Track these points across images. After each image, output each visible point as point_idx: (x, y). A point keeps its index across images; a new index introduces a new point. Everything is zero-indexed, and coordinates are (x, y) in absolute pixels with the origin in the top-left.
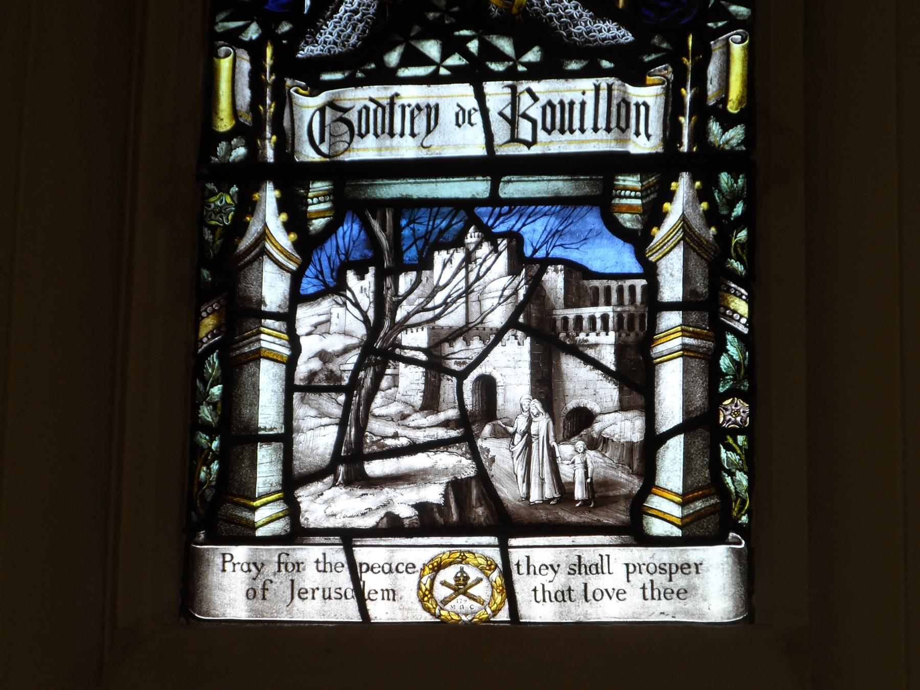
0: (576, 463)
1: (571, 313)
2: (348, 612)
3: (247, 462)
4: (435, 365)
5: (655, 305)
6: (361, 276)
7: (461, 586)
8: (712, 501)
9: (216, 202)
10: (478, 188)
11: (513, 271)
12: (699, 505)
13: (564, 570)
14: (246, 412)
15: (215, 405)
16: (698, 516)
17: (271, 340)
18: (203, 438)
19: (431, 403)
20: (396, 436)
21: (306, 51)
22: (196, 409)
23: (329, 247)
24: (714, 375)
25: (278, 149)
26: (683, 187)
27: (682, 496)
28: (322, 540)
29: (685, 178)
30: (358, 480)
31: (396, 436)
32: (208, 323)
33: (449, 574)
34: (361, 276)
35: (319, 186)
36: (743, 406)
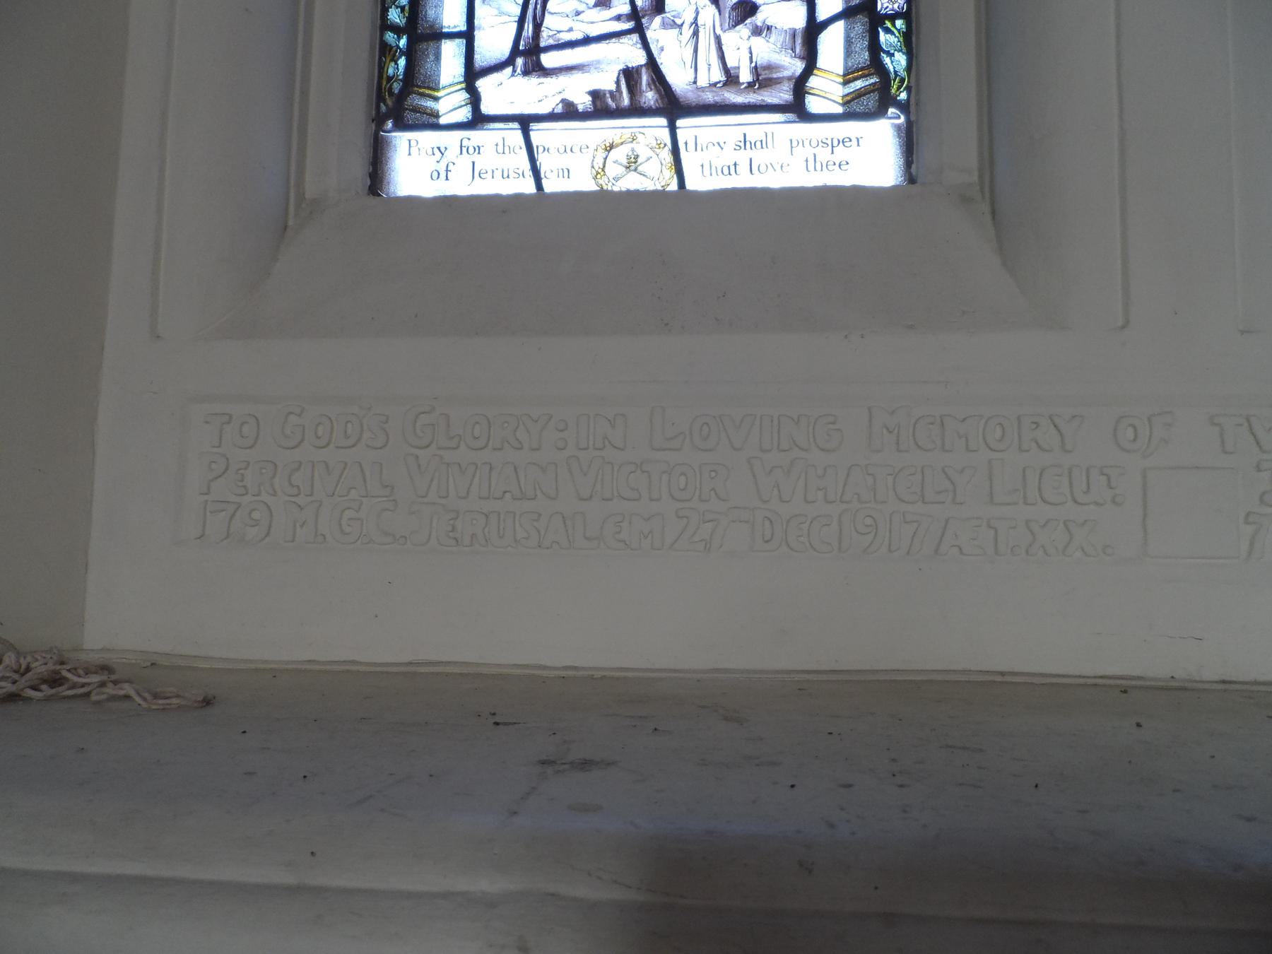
0: (743, 49)
3: (432, 57)
7: (632, 164)
8: (872, 81)
12: (859, 84)
13: (729, 147)
14: (431, 13)
15: (403, 9)
16: (859, 94)
18: (390, 37)
20: (571, 30)
22: (385, 11)
27: (844, 75)
28: (501, 125)
30: (535, 68)
31: (571, 30)
33: (620, 154)
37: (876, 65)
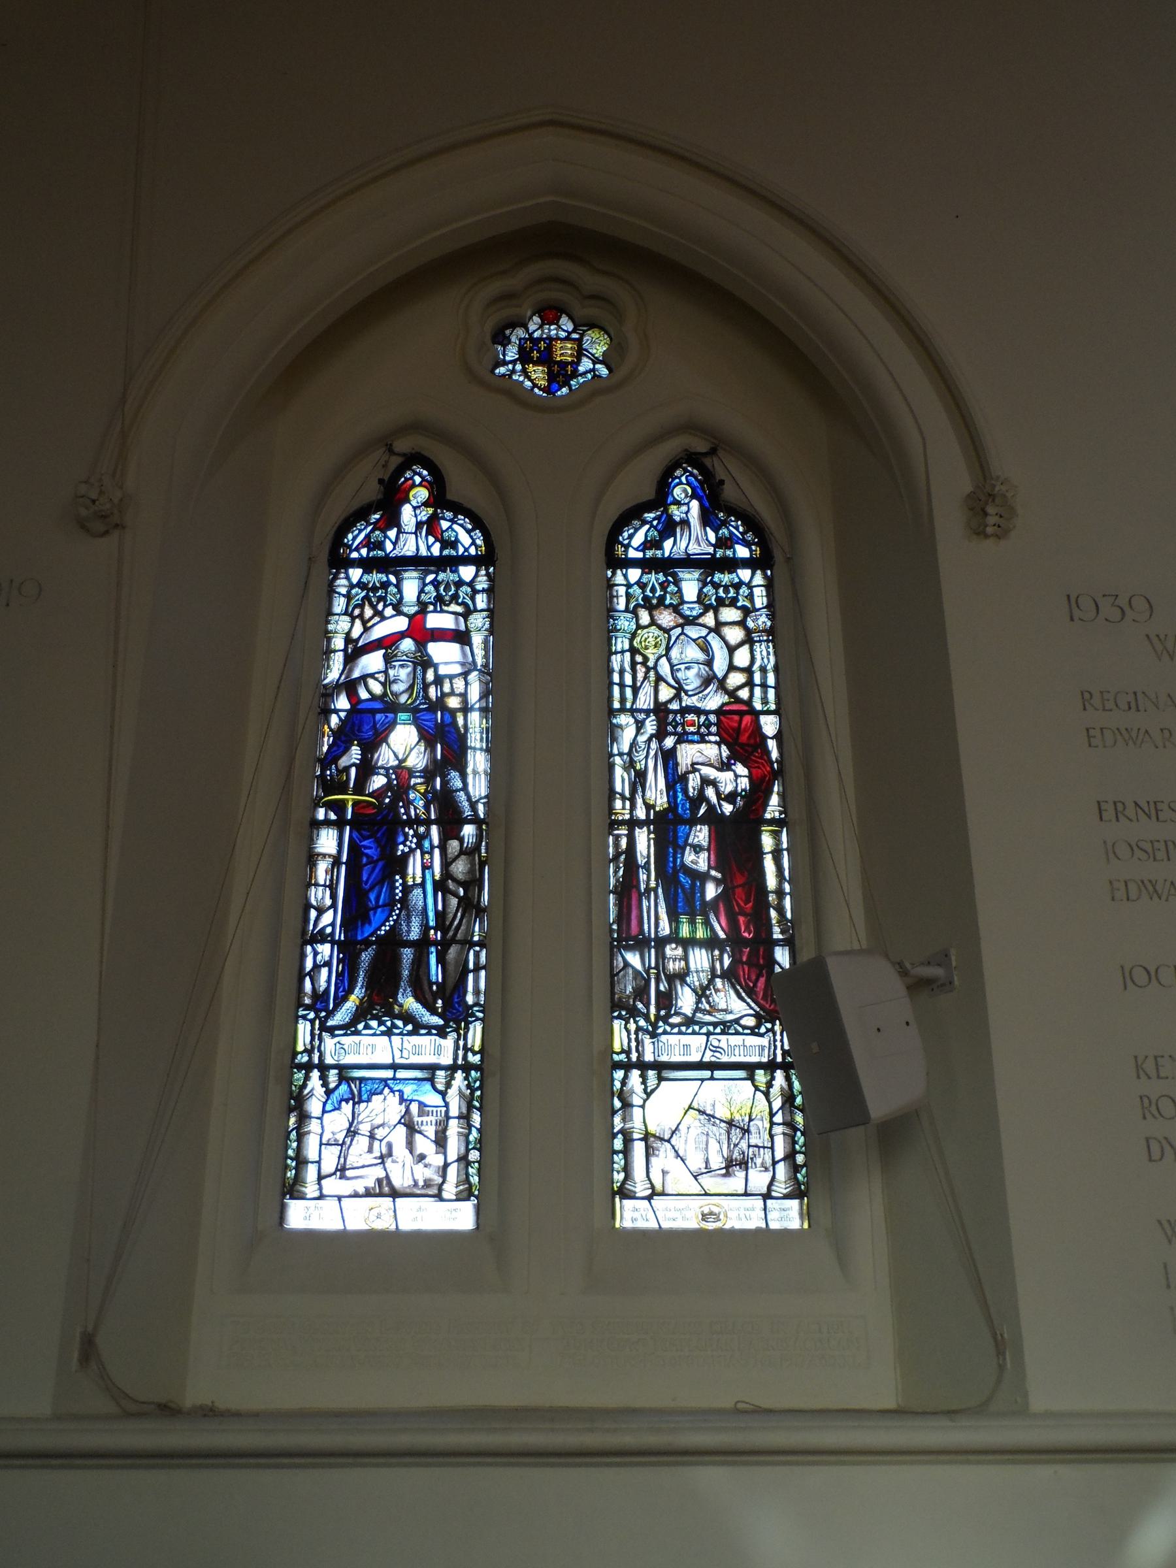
0: (422, 1173)
1: (420, 1119)
2: (338, 1226)
4: (372, 1137)
5: (448, 1117)
6: (347, 1102)
9: (296, 1076)
10: (388, 1074)
11: (401, 1104)
16: (461, 1192)
17: (314, 1126)
18: (289, 1161)
19: (370, 1150)
21: (330, 1023)
23: (336, 1093)
24: (468, 1143)
25: (320, 1057)
26: (459, 1075)
29: (460, 1072)
32: (292, 1120)
34: (347, 1102)
35: (334, 1072)
36: (477, 1153)
37: (467, 1181)
